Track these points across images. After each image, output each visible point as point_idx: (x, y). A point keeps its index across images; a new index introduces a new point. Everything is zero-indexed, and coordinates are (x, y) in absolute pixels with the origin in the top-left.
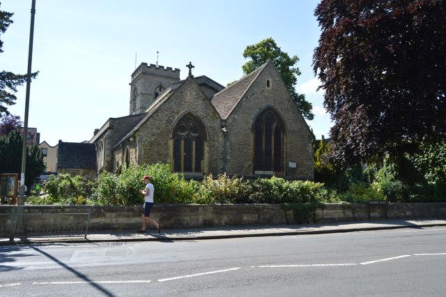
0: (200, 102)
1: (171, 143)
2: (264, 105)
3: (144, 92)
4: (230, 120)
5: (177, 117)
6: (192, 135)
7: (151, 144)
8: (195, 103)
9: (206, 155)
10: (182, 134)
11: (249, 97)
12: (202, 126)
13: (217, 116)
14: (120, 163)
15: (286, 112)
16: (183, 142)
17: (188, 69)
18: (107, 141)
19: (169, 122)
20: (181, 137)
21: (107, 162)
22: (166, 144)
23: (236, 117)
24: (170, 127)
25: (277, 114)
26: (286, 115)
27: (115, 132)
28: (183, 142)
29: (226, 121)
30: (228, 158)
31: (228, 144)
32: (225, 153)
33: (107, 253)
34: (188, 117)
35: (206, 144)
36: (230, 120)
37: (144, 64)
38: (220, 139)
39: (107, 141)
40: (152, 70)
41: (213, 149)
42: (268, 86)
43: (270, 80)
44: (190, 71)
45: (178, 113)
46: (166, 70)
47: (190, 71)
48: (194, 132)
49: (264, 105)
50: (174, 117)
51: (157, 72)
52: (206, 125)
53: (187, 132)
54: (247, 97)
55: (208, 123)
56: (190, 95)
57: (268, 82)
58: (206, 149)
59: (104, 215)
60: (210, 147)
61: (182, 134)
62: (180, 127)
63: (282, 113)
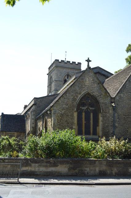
0: (96, 85)
1: (75, 115)
3: (56, 79)
4: (117, 98)
5: (79, 96)
6: (91, 108)
7: (62, 115)
8: (93, 86)
9: (101, 123)
10: (83, 108)
12: (97, 102)
13: (108, 95)
14: (41, 128)
16: (84, 114)
17: (87, 63)
18: (32, 113)
19: (74, 99)
20: (83, 110)
21: (33, 127)
22: (72, 115)
23: (122, 95)
24: (75, 104)
27: (38, 107)
28: (84, 114)
29: (114, 98)
30: (117, 125)
31: (116, 115)
32: (114, 121)
33: (33, 193)
34: (88, 96)
35: (100, 115)
36: (117, 98)
37: (57, 61)
38: (111, 112)
39: (32, 113)
40: (62, 64)
41: (105, 118)
44: (88, 64)
45: (80, 94)
46: (71, 64)
47: (88, 64)
48: (92, 107)
51: (66, 65)
53: (87, 107)
55: (101, 100)
56: (88, 81)
58: (101, 119)
59: (30, 165)
60: (103, 117)
61: (83, 108)
62: (82, 103)
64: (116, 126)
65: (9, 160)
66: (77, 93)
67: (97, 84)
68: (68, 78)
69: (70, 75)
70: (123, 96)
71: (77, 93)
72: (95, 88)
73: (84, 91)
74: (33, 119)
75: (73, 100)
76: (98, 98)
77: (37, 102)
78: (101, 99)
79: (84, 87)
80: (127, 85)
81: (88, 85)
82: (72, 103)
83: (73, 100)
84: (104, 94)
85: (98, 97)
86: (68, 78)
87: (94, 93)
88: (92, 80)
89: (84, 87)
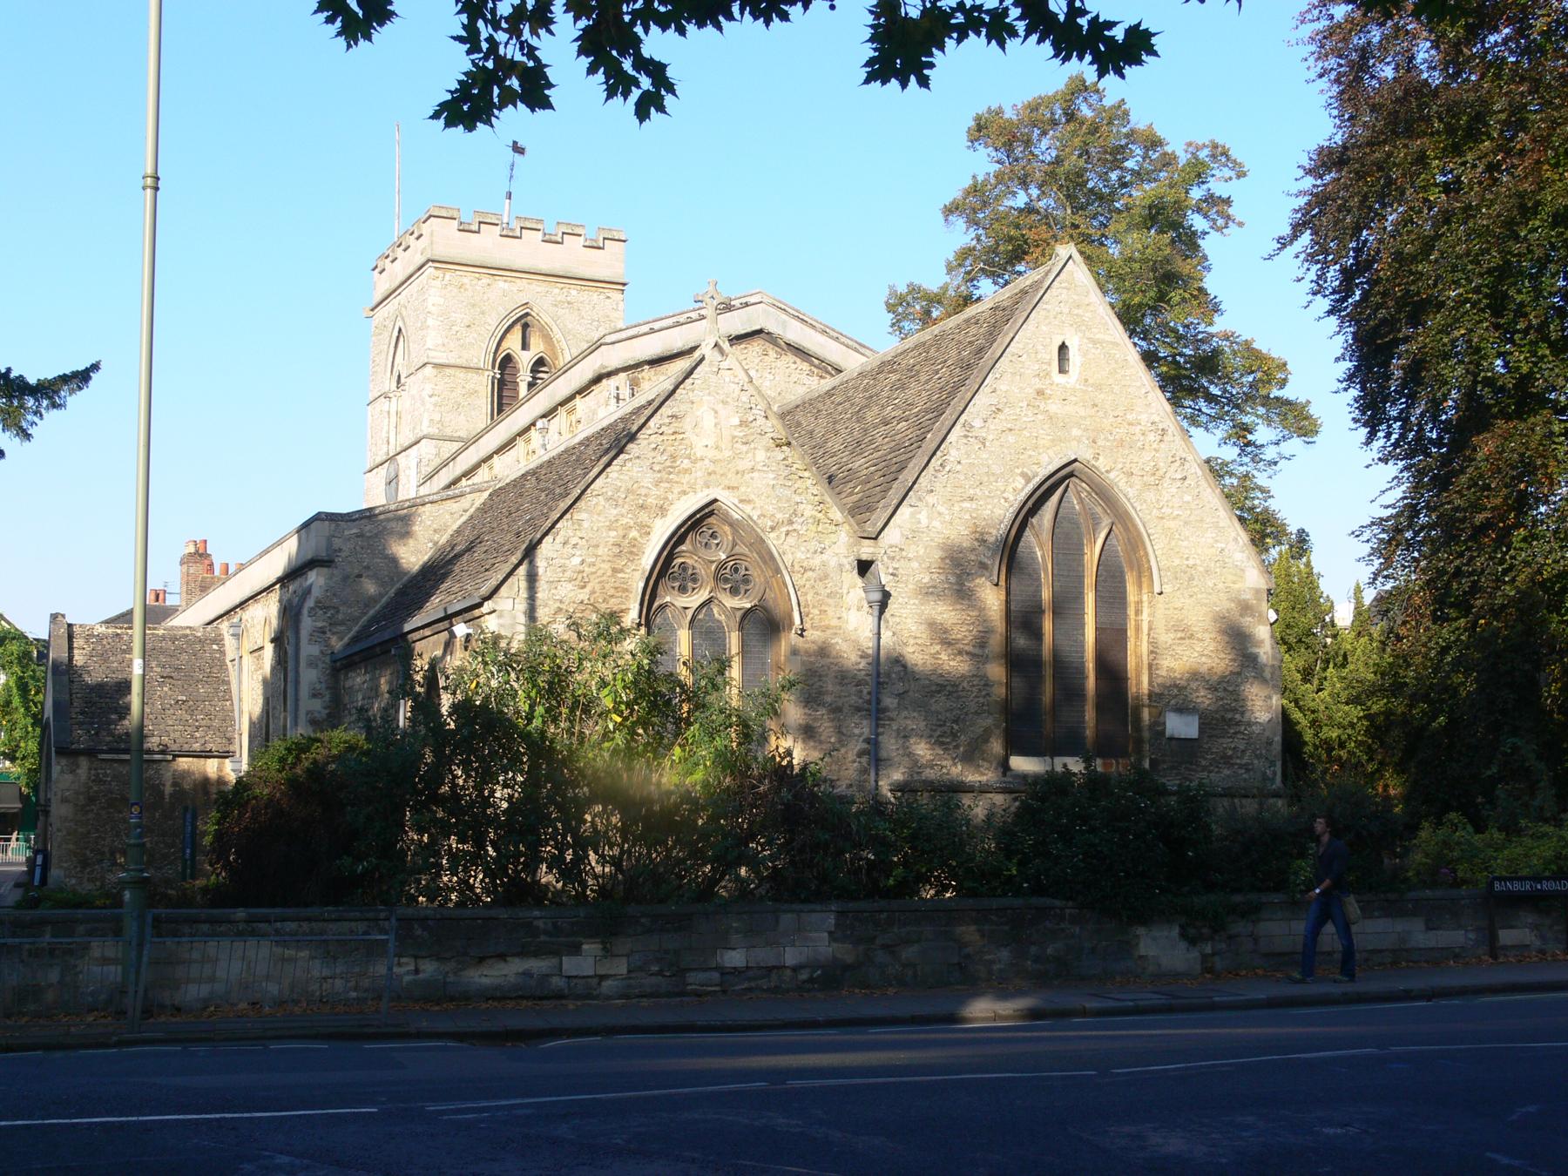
0: (761, 455)
6: (731, 602)
8: (744, 464)
11: (977, 423)
15: (1147, 485)
25: (1104, 494)
26: (1150, 496)
27: (346, 578)
45: (662, 511)
48: (734, 591)
49: (1048, 463)
50: (646, 530)
52: (788, 559)
53: (703, 595)
54: (968, 427)
57: (1063, 348)
63: (1128, 491)
64: (885, 710)
65: (305, 925)
68: (525, 346)
69: (545, 318)
70: (930, 518)
72: (755, 475)
73: (684, 493)
74: (312, 664)
75: (619, 555)
76: (772, 535)
77: (337, 543)
79: (686, 471)
80: (953, 452)
81: (711, 454)
82: (615, 570)
83: (619, 555)
84: (809, 511)
85: (773, 529)
86: (525, 346)
87: (748, 509)
88: (736, 421)
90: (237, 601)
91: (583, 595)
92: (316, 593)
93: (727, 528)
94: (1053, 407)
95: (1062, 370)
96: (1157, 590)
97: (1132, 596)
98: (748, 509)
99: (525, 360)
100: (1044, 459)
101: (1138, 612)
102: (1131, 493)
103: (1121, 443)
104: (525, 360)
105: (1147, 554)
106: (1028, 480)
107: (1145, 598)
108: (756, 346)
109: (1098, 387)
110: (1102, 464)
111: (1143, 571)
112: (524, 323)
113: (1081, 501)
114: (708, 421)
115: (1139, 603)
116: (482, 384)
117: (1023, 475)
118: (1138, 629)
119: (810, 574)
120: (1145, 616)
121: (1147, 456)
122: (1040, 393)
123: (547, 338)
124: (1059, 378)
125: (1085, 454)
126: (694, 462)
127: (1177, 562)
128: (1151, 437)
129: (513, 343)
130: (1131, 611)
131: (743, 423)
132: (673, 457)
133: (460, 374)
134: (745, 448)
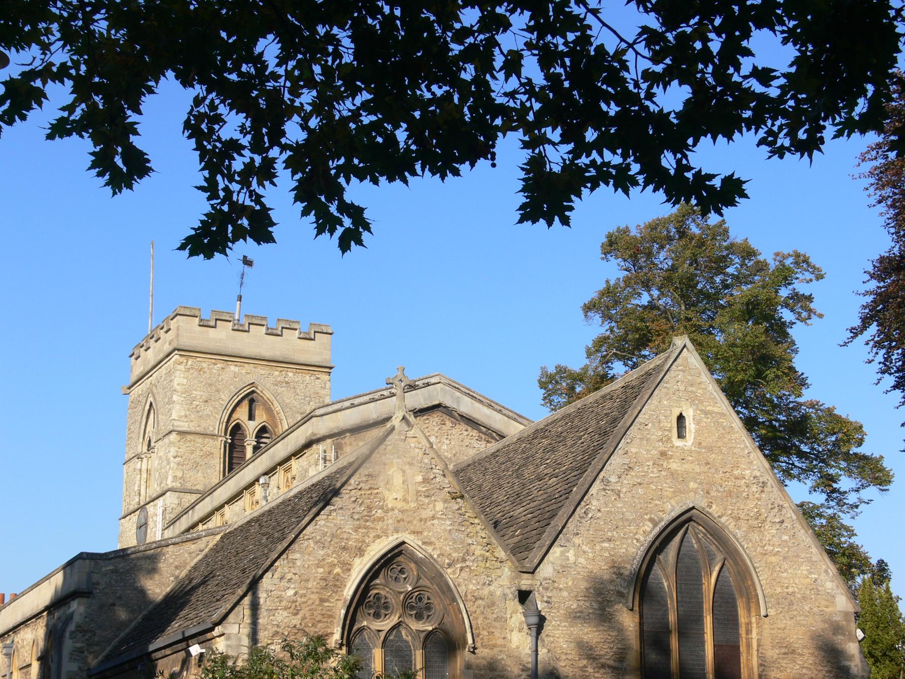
0: (440, 506)
2: (668, 507)
6: (416, 626)
11: (613, 479)
15: (752, 528)
25: (717, 535)
26: (755, 536)
42: (681, 436)
43: (689, 414)
48: (419, 617)
49: (671, 510)
50: (347, 568)
52: (462, 589)
53: (394, 620)
54: (606, 482)
57: (681, 418)
63: (736, 531)
66: (344, 548)
67: (445, 501)
68: (251, 417)
69: (268, 395)
70: (576, 556)
71: (344, 548)
72: (436, 522)
73: (379, 537)
75: (325, 588)
76: (449, 571)
77: (96, 577)
78: (464, 574)
79: (381, 519)
80: (594, 502)
81: (400, 505)
82: (322, 600)
83: (325, 588)
84: (479, 551)
85: (450, 565)
86: (251, 417)
87: (429, 549)
88: (419, 478)
89: (381, 519)
90: (11, 626)
91: (296, 621)
92: (77, 619)
93: (413, 565)
94: (674, 466)
95: (681, 436)
96: (763, 613)
97: (743, 620)
98: (429, 549)
99: (251, 428)
100: (668, 507)
101: (748, 632)
102: (739, 534)
103: (730, 494)
104: (251, 428)
105: (753, 584)
106: (655, 524)
107: (754, 620)
108: (435, 419)
109: (710, 449)
110: (715, 510)
111: (751, 598)
112: (251, 399)
113: (699, 541)
114: (398, 480)
115: (749, 624)
116: (217, 447)
117: (651, 520)
118: (749, 645)
119: (480, 602)
120: (754, 635)
121: (751, 504)
122: (663, 454)
123: (269, 411)
124: (678, 443)
125: (701, 503)
126: (387, 512)
127: (779, 590)
128: (754, 488)
129: (242, 414)
130: (742, 631)
131: (426, 481)
132: (370, 509)
133: (199, 440)
134: (426, 500)
